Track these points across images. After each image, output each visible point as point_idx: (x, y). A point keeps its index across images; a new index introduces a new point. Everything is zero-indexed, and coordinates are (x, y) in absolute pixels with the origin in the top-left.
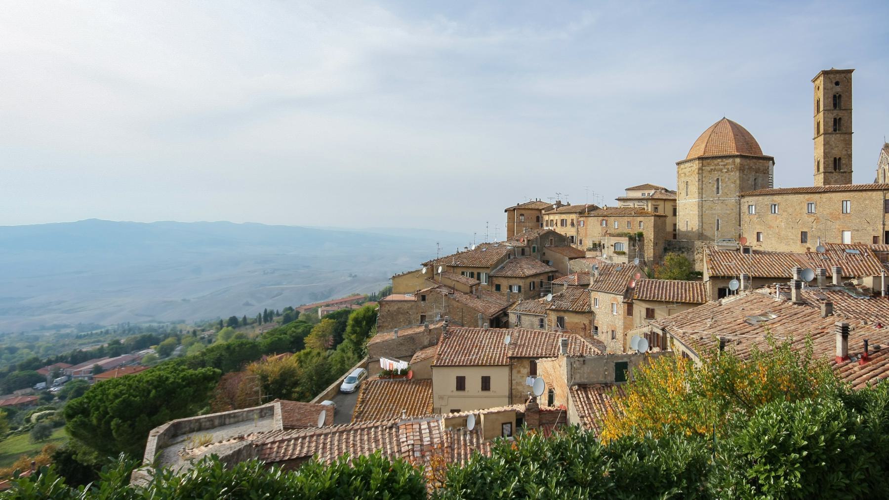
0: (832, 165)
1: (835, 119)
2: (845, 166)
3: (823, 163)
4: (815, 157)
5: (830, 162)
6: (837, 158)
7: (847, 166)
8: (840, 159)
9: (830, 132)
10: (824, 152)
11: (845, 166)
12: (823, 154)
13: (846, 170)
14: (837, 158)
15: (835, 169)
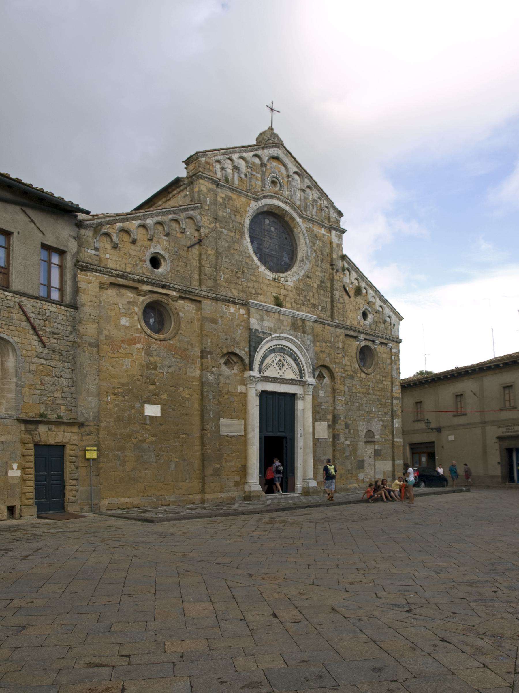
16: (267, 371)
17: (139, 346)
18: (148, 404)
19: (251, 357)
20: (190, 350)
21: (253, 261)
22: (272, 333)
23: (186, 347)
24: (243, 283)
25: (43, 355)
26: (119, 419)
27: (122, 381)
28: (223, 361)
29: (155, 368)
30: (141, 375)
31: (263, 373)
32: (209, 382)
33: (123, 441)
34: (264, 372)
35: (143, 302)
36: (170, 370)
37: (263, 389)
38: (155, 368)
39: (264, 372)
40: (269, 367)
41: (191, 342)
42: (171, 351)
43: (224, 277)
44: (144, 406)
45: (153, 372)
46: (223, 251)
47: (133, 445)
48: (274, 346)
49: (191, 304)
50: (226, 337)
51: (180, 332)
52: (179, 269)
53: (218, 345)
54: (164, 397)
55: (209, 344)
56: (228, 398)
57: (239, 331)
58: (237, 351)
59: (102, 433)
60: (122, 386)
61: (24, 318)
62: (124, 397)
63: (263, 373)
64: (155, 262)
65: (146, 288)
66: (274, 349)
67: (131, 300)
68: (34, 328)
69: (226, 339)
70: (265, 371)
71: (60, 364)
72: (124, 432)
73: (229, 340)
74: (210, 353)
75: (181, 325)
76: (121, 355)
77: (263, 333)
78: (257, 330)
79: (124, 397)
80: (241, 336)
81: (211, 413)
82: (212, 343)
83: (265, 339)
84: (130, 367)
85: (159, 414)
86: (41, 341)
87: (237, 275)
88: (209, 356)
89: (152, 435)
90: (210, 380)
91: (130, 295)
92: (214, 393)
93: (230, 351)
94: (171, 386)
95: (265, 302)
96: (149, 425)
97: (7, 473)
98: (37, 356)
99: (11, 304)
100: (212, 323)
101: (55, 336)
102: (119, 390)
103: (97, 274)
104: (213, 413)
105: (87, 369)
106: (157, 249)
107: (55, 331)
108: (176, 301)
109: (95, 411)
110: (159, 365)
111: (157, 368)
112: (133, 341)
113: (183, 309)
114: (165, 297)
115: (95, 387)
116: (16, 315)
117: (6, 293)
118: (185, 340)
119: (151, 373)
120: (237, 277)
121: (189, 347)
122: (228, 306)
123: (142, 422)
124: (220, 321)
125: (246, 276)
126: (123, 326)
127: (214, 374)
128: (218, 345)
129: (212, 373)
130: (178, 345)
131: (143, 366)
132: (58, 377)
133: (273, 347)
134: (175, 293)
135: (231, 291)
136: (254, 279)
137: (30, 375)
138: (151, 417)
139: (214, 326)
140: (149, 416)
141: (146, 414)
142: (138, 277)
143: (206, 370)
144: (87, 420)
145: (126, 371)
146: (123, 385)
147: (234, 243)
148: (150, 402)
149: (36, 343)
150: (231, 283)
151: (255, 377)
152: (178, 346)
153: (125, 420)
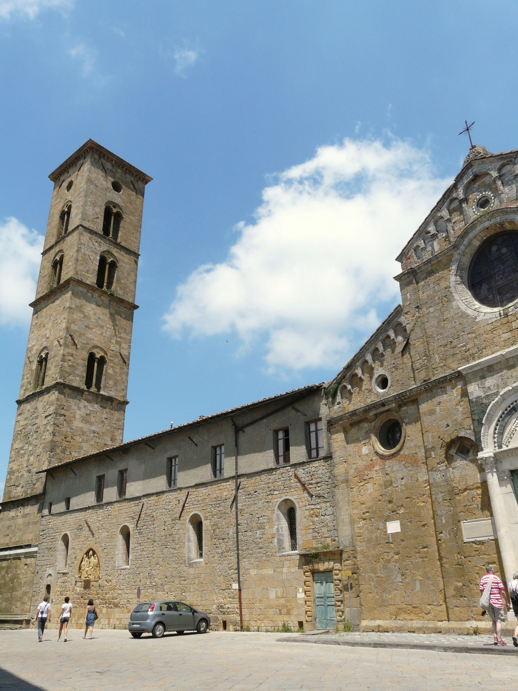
0: (82, 371)
1: (103, 261)
2: (111, 382)
3: (59, 358)
4: (29, 350)
5: (80, 362)
6: (98, 356)
7: (116, 384)
8: (102, 361)
9: (88, 282)
10: (68, 329)
11: (111, 382)
12: (63, 334)
13: (112, 394)
14: (98, 356)
15: (88, 383)
16: (511, 441)
17: (377, 468)
18: (389, 521)
19: (477, 433)
20: (419, 453)
21: (468, 316)
22: (500, 390)
23: (414, 451)
24: (461, 349)
25: (312, 502)
26: (369, 541)
27: (369, 504)
28: (455, 451)
29: (391, 485)
30: (381, 495)
31: (507, 446)
32: (436, 483)
33: (374, 563)
34: (507, 444)
35: (374, 426)
36: (403, 482)
37: (513, 468)
38: (391, 485)
39: (507, 444)
40: (513, 434)
41: (418, 444)
42: (402, 461)
43: (439, 357)
44: (386, 524)
45: (389, 489)
46: (433, 331)
47: (381, 565)
48: (512, 404)
49: (413, 405)
50: (447, 423)
51: (406, 439)
52: (398, 378)
53: (439, 437)
54: (402, 511)
55: (430, 439)
56: (468, 494)
57: (461, 409)
58: (462, 434)
59: (359, 557)
60: (369, 509)
61: (296, 480)
62: (370, 520)
63: (507, 446)
64: (383, 382)
65: (372, 413)
66: (513, 407)
67: (367, 429)
68: (303, 485)
69: (448, 426)
70: (509, 442)
71: (324, 505)
72: (374, 554)
73: (451, 425)
74: (433, 448)
75: (407, 431)
76: (367, 481)
77: (487, 397)
78: (478, 397)
79: (370, 520)
80: (463, 414)
81: (443, 518)
82: (433, 437)
83: (490, 403)
84: (372, 490)
85: (400, 531)
86: (309, 493)
87: (452, 346)
88: (433, 453)
89: (398, 554)
90: (437, 479)
91: (366, 425)
92: (443, 494)
93: (453, 437)
94: (406, 498)
95: (493, 353)
96: (392, 543)
97: (296, 595)
98: (309, 505)
99: (291, 473)
100: (430, 415)
101: (319, 485)
102: (368, 514)
103: (340, 422)
104: (445, 518)
105: (341, 503)
106: (379, 371)
107: (319, 480)
108: (400, 410)
109: (350, 537)
110: (393, 480)
111: (392, 483)
112: (372, 466)
113: (406, 415)
114: (389, 413)
115: (347, 517)
116: (294, 480)
117: (287, 468)
118: (412, 445)
119: (388, 490)
120: (453, 348)
121: (417, 450)
122: (444, 388)
123: (386, 541)
124: (438, 409)
125: (463, 339)
126: (365, 455)
127: (441, 471)
128: (439, 437)
129: (438, 471)
130: (407, 453)
131: (381, 485)
132: (324, 516)
133: (512, 406)
134: (394, 405)
135: (449, 368)
136: (474, 335)
137: (305, 520)
138: (393, 535)
139: (433, 417)
140: (391, 533)
141: (389, 532)
142: (361, 409)
143: (431, 470)
144: (345, 547)
145: (370, 495)
146: (369, 508)
147: (442, 313)
148: (389, 519)
149: (307, 495)
150: (447, 358)
151: (483, 458)
152: (407, 454)
153: (373, 541)
